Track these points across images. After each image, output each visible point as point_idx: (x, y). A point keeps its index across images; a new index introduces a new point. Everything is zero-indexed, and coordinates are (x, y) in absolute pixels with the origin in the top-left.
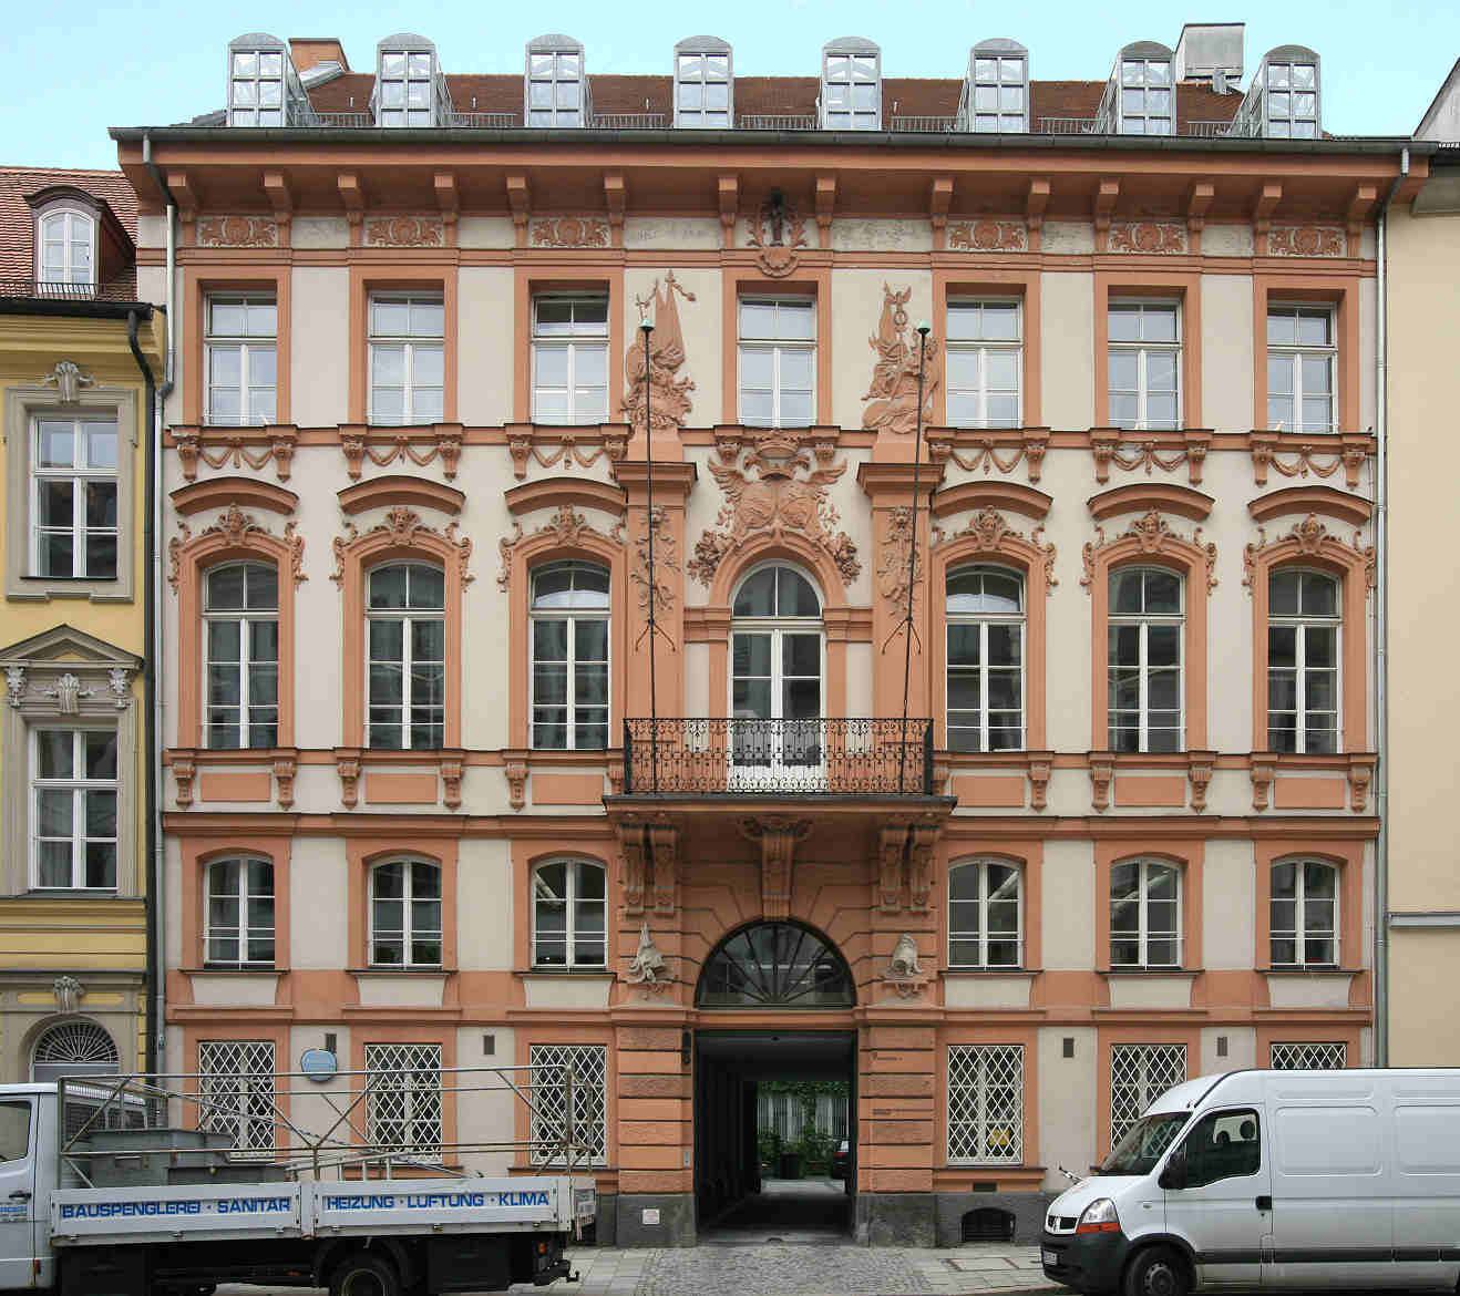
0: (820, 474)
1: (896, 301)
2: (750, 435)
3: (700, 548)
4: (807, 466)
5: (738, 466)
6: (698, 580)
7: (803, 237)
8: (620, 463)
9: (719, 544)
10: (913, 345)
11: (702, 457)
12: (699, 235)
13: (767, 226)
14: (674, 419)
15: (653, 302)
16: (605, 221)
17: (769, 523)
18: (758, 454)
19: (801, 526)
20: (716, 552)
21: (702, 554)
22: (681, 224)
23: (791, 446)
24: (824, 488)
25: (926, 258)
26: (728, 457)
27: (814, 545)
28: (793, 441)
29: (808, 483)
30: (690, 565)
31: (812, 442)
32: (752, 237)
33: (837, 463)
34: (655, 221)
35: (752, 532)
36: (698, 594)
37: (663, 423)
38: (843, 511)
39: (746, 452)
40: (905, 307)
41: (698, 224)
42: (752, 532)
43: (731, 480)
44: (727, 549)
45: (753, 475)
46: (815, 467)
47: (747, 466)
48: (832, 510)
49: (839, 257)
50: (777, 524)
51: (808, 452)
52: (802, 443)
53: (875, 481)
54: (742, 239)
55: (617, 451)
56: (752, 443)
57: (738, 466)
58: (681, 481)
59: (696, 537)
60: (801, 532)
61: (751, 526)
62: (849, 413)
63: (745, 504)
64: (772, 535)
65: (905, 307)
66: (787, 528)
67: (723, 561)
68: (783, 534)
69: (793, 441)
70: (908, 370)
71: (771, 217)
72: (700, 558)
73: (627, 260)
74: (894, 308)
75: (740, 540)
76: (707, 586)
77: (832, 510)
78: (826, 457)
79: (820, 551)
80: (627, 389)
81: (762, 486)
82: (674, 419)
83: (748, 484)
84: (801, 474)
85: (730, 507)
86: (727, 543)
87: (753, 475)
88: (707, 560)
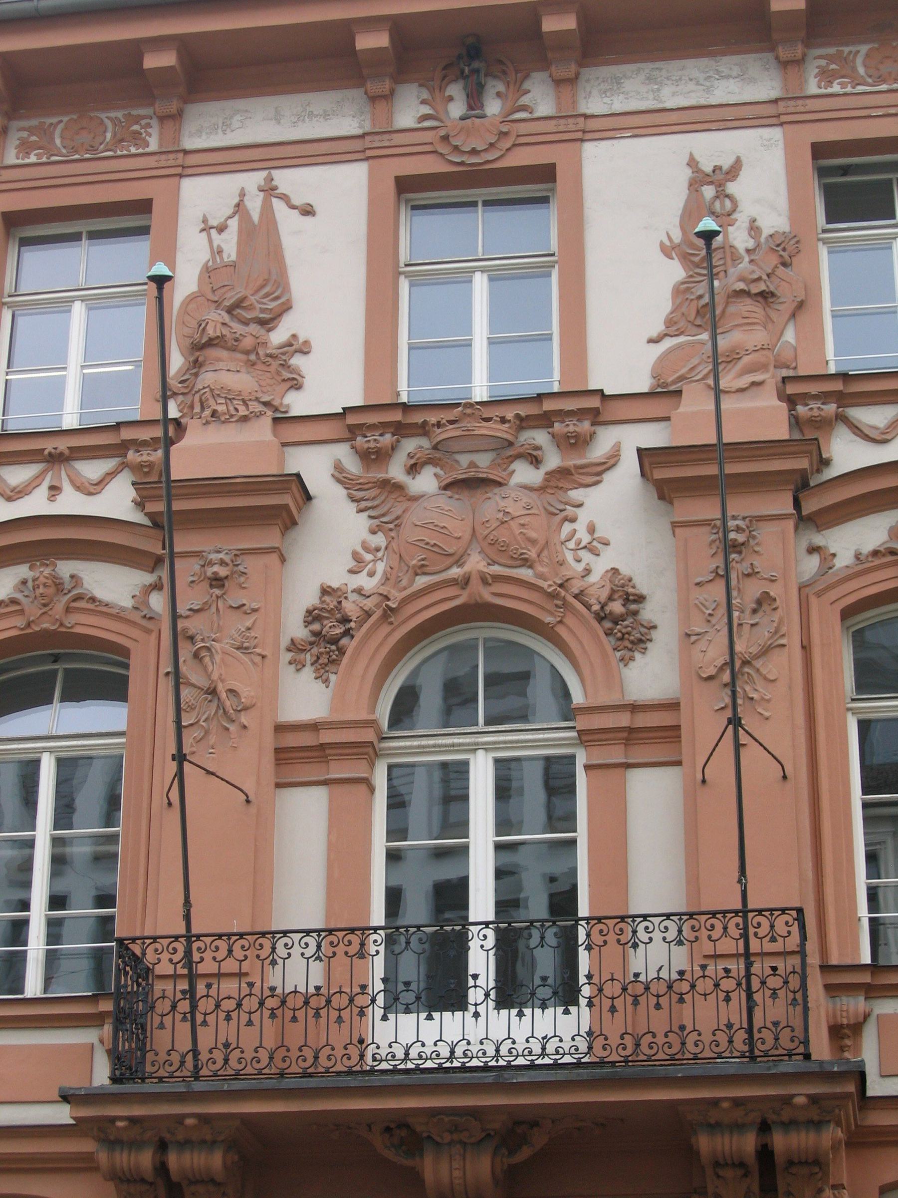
0: (563, 473)
1: (712, 185)
2: (418, 418)
3: (312, 616)
4: (536, 461)
5: (396, 471)
6: (308, 672)
7: (525, 100)
8: (154, 485)
9: (350, 607)
10: (751, 244)
11: (316, 465)
12: (336, 116)
13: (456, 90)
14: (265, 404)
15: (234, 224)
16: (148, 111)
17: (459, 563)
18: (435, 447)
19: (526, 562)
20: (345, 620)
21: (316, 627)
22: (290, 104)
23: (502, 431)
24: (576, 494)
25: (771, 110)
26: (374, 457)
27: (552, 596)
28: (503, 420)
29: (541, 489)
30: (294, 646)
31: (545, 420)
32: (426, 110)
33: (600, 449)
34: (241, 104)
35: (422, 581)
36: (305, 698)
37: (243, 411)
38: (615, 527)
39: (410, 445)
40: (732, 188)
41: (320, 101)
42: (422, 581)
43: (375, 493)
44: (368, 614)
45: (426, 482)
46: (553, 460)
47: (413, 469)
48: (591, 529)
49: (592, 124)
50: (475, 563)
51: (540, 437)
52: (524, 423)
53: (670, 476)
54: (409, 111)
55: (151, 465)
56: (423, 430)
57: (396, 471)
58: (277, 506)
59: (301, 594)
60: (525, 573)
61: (421, 570)
62: (621, 360)
63: (410, 534)
64: (465, 582)
65: (732, 188)
66: (496, 569)
67: (359, 635)
68: (485, 580)
69: (503, 420)
70: (741, 286)
71: (462, 76)
72: (316, 634)
73: (187, 165)
74: (709, 192)
75: (396, 596)
76: (326, 681)
77: (591, 529)
78: (575, 443)
79: (565, 604)
80: (177, 361)
81: (444, 501)
82: (265, 404)
83: (415, 499)
84: (524, 474)
85: (379, 540)
86: (369, 604)
87: (426, 482)
88: (328, 638)
